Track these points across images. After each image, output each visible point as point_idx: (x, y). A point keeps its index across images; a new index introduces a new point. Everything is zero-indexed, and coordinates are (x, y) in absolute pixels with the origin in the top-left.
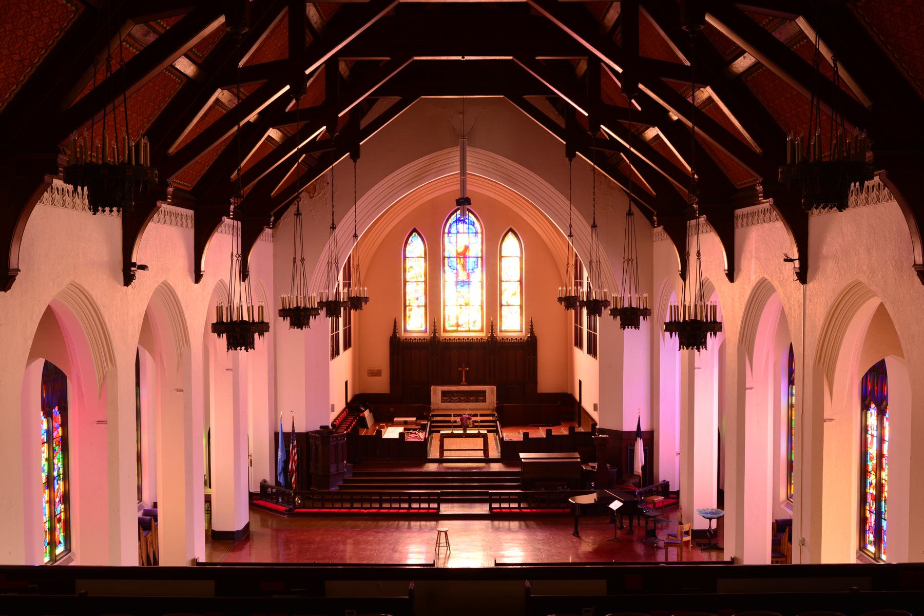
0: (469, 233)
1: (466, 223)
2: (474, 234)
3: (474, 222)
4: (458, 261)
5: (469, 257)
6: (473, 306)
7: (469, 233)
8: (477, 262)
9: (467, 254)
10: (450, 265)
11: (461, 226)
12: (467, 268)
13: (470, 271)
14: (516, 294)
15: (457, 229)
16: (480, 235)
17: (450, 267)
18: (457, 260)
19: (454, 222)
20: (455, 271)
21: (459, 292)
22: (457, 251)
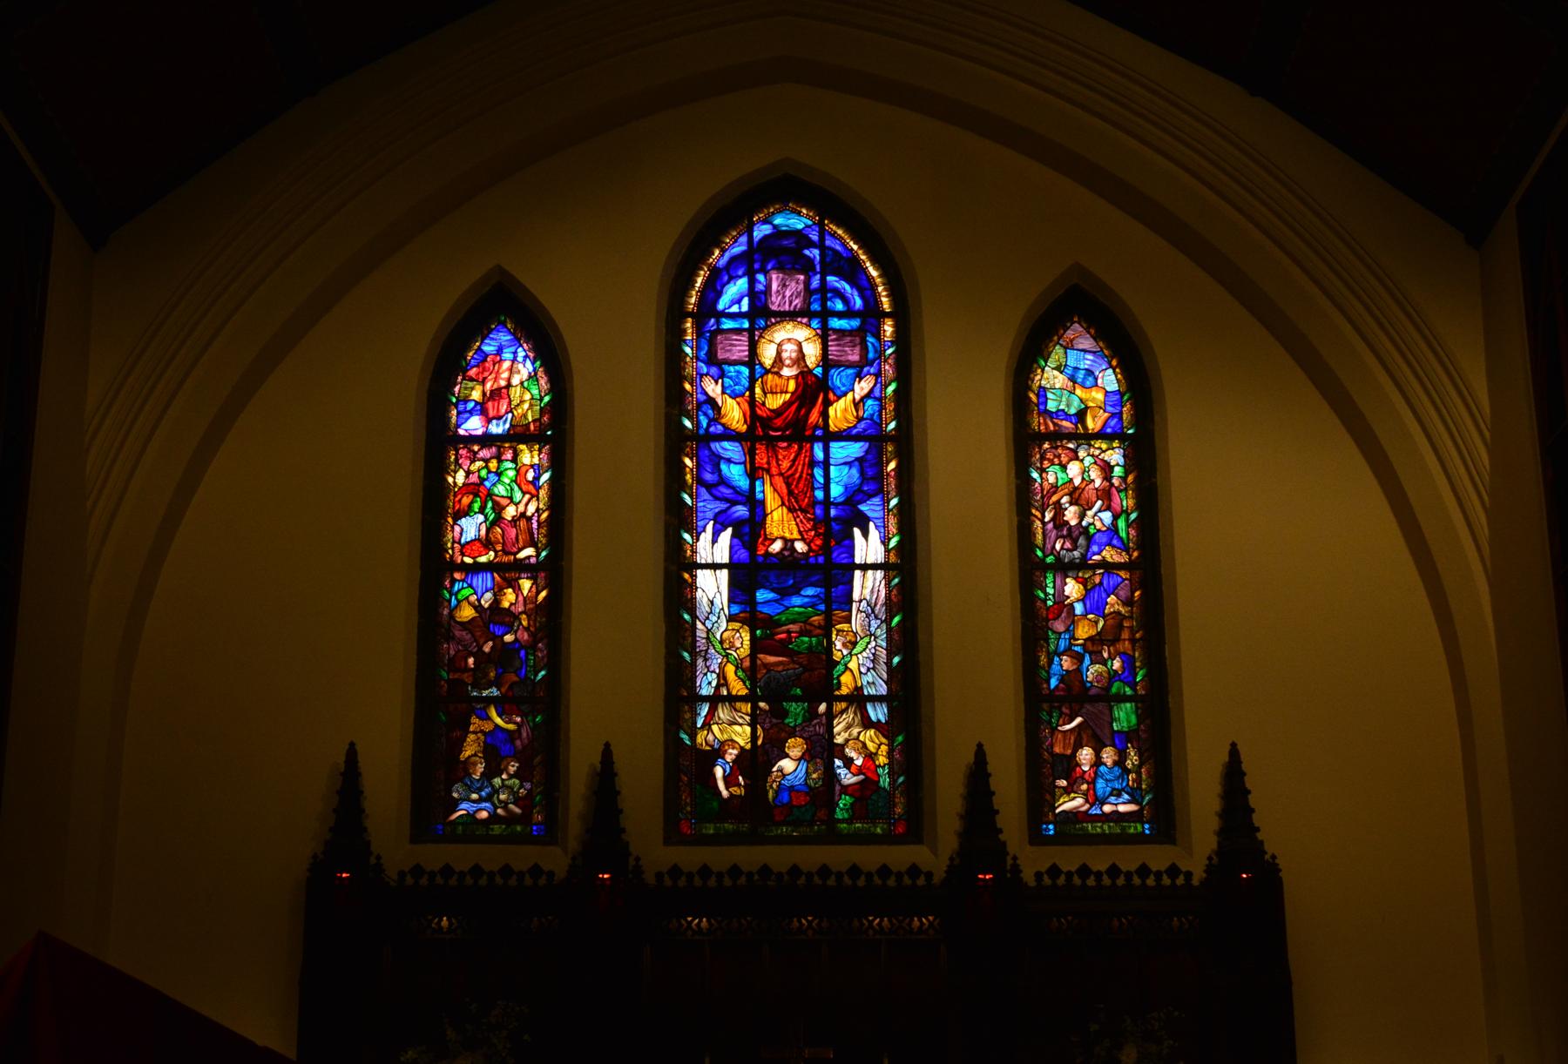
0: (825, 315)
1: (807, 267)
2: (855, 323)
3: (854, 259)
4: (761, 458)
5: (829, 437)
6: (858, 699)
7: (825, 315)
8: (880, 465)
9: (814, 416)
10: (708, 477)
11: (784, 290)
12: (819, 494)
13: (833, 512)
14: (1125, 635)
15: (752, 293)
16: (888, 328)
17: (710, 487)
18: (751, 453)
19: (734, 260)
20: (741, 511)
21: (771, 623)
22: (752, 401)
